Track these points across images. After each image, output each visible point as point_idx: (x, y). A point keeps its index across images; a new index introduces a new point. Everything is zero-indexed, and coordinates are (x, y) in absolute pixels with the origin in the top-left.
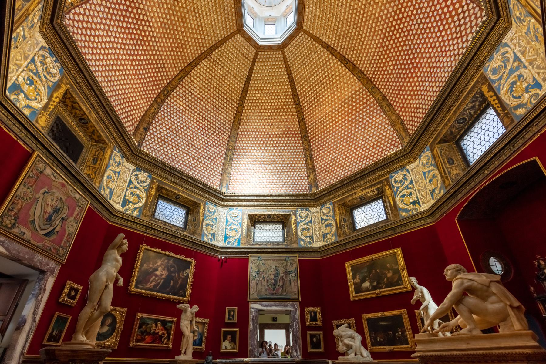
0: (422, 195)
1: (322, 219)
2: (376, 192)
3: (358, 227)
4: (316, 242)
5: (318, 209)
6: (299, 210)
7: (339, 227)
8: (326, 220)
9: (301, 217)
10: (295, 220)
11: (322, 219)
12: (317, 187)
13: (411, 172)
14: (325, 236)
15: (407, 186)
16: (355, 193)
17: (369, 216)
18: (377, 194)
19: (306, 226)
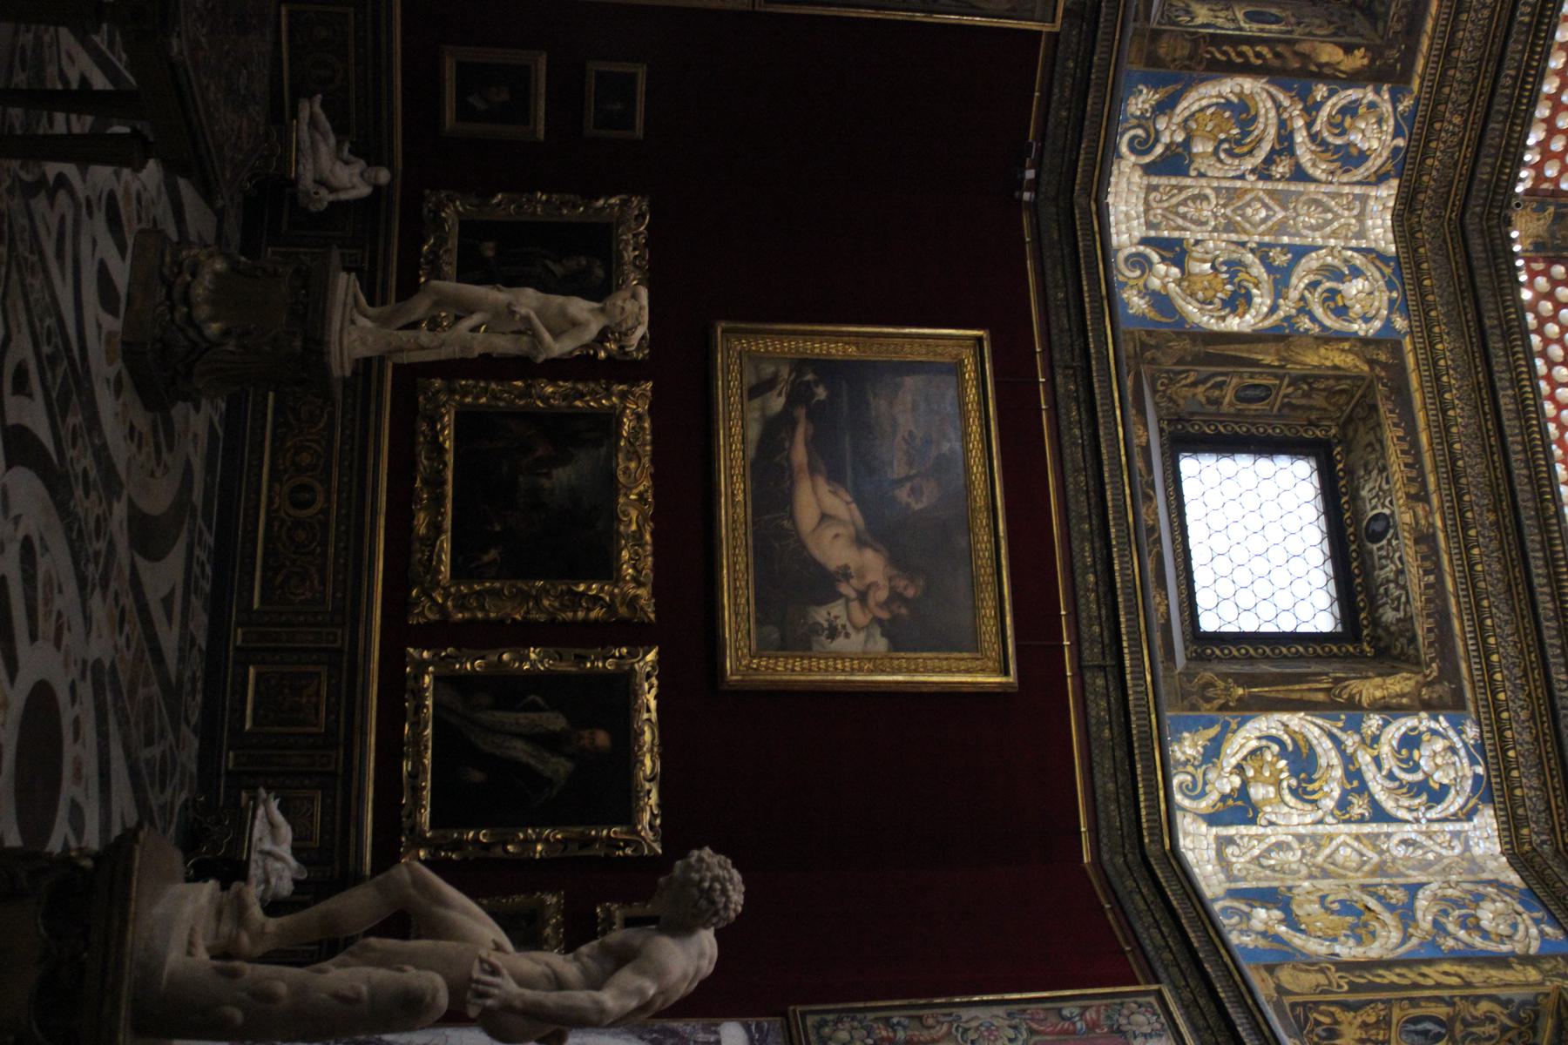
0: (1288, 847)
1: (1300, 252)
2: (1389, 615)
3: (1189, 465)
4: (1151, 188)
5: (1380, 232)
6: (1406, 104)
7: (1214, 349)
8: (1281, 279)
9: (1350, 110)
11: (1300, 252)
12: (1547, 251)
13: (1450, 827)
14: (1175, 252)
15: (1363, 789)
16: (1421, 497)
17: (1252, 541)
18: (1375, 622)
19: (1272, 131)
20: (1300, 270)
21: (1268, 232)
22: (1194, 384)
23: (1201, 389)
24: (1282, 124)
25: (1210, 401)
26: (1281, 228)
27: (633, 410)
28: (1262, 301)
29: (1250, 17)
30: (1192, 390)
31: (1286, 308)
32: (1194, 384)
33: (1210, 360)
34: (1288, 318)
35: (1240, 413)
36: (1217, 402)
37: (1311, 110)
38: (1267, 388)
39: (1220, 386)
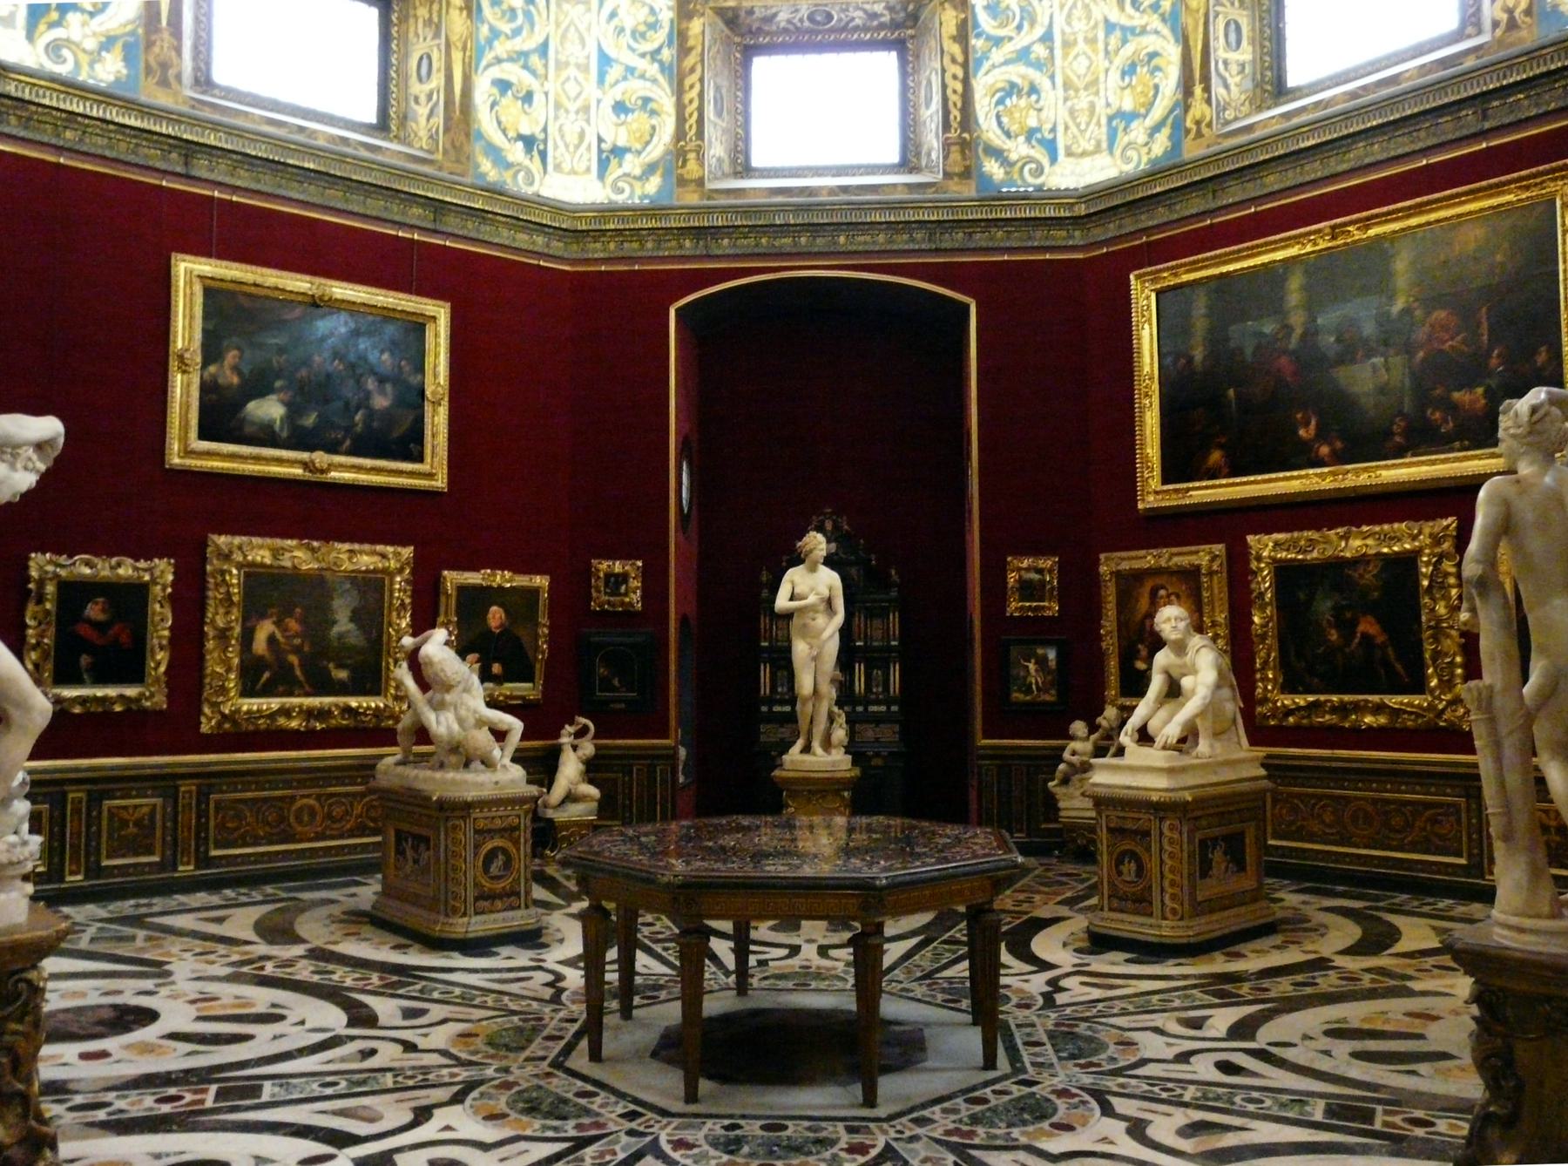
8: (1128, 32)
10: (962, 36)
20: (1124, 21)
21: (1095, 51)
22: (1227, 87)
23: (1231, 81)
24: (1006, 63)
25: (1242, 71)
26: (1091, 41)
27: (1265, 547)
28: (1150, 43)
29: (927, 106)
30: (1233, 88)
31: (1155, 22)
32: (1227, 87)
33: (1206, 79)
34: (1164, 20)
35: (1252, 42)
36: (1243, 66)
37: (998, 42)
38: (1227, 25)
39: (1226, 63)
